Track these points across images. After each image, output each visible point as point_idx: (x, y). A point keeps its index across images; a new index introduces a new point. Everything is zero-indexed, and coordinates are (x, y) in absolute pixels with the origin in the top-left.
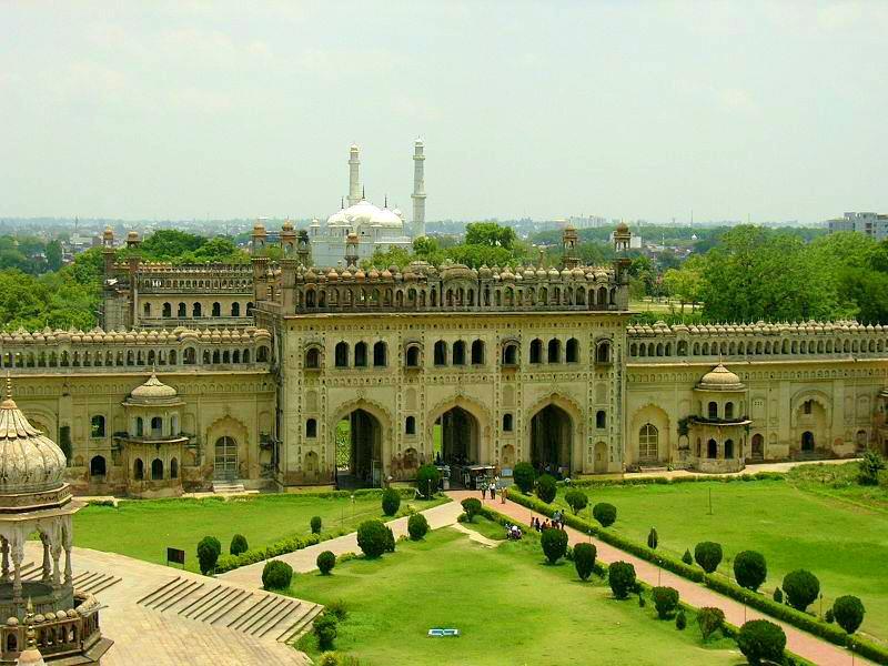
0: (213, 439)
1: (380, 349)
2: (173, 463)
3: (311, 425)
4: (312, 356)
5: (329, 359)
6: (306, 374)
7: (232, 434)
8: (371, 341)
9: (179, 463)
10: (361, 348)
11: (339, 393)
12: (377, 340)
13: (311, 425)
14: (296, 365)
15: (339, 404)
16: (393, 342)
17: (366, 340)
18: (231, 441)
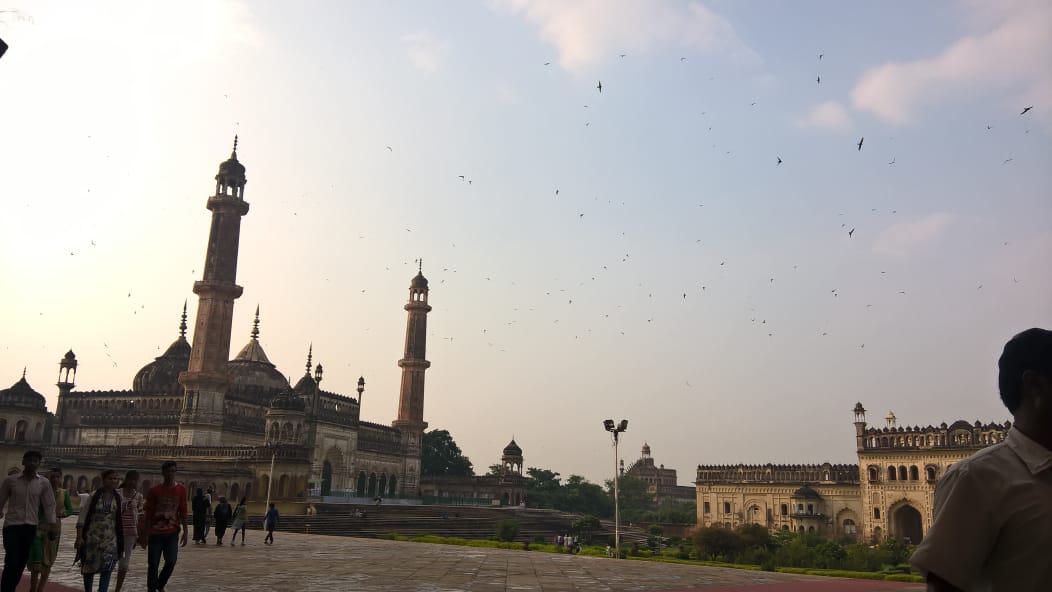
0: (842, 520)
1: (914, 470)
2: (811, 528)
3: (877, 511)
4: (874, 472)
5: (884, 476)
6: (871, 482)
7: (851, 518)
8: (908, 465)
9: (816, 528)
10: (903, 469)
11: (890, 495)
12: (911, 464)
13: (877, 511)
14: (866, 477)
15: (892, 501)
16: (921, 464)
17: (905, 464)
18: (853, 523)
